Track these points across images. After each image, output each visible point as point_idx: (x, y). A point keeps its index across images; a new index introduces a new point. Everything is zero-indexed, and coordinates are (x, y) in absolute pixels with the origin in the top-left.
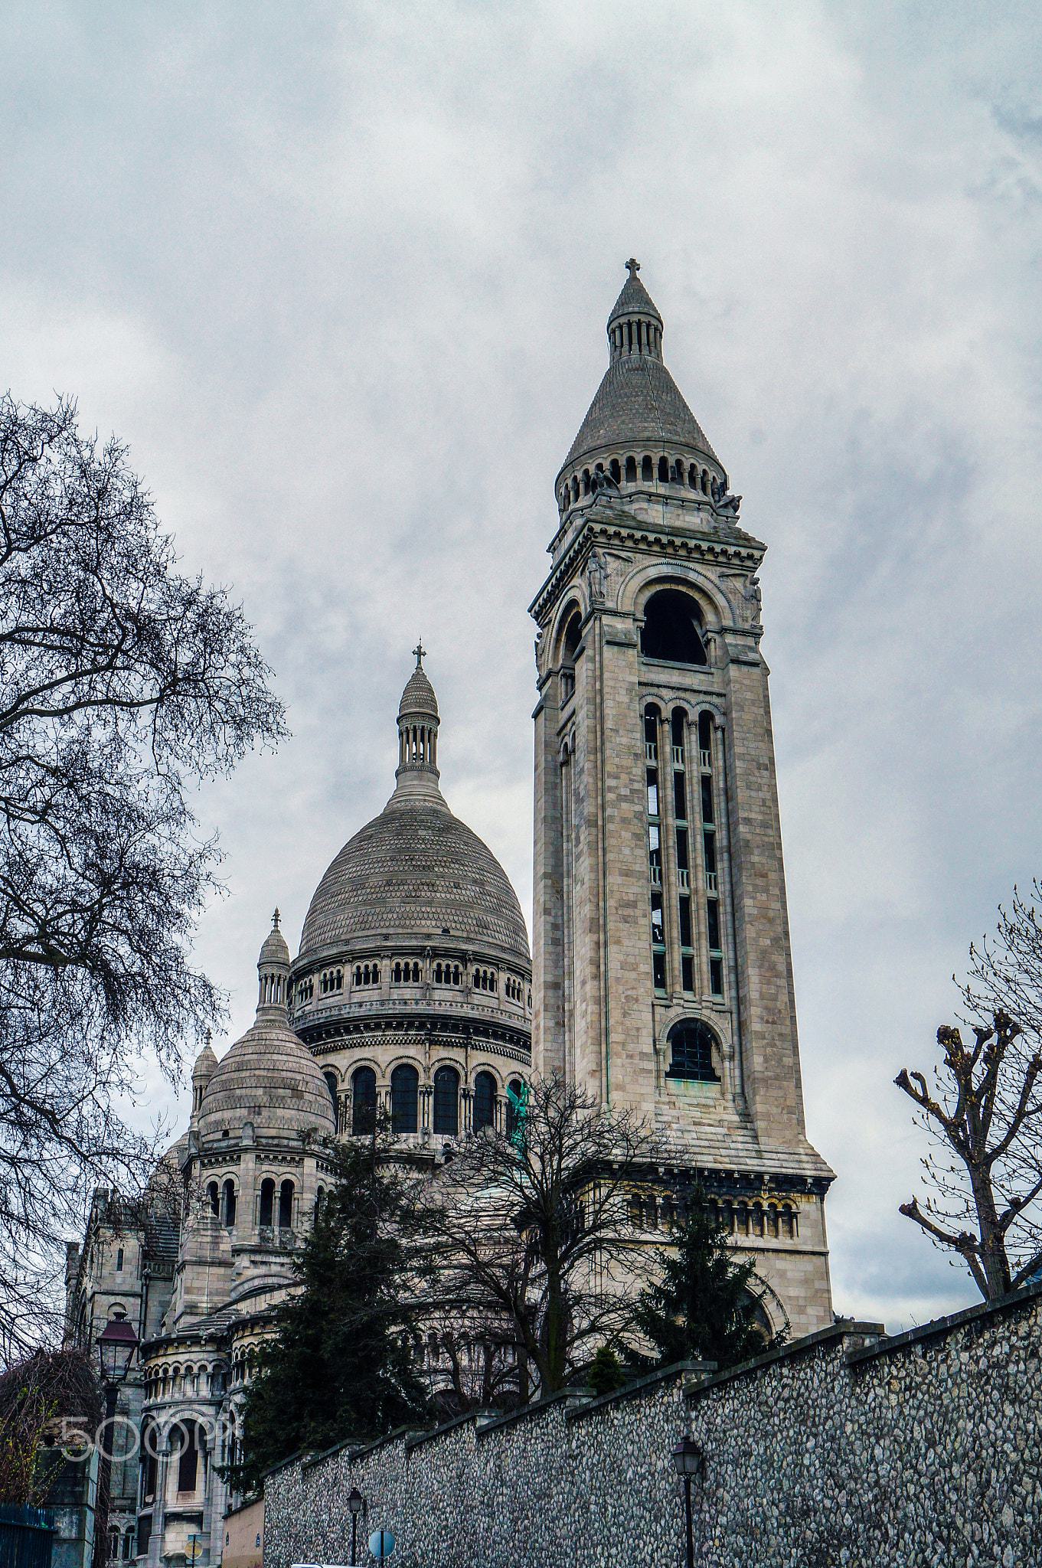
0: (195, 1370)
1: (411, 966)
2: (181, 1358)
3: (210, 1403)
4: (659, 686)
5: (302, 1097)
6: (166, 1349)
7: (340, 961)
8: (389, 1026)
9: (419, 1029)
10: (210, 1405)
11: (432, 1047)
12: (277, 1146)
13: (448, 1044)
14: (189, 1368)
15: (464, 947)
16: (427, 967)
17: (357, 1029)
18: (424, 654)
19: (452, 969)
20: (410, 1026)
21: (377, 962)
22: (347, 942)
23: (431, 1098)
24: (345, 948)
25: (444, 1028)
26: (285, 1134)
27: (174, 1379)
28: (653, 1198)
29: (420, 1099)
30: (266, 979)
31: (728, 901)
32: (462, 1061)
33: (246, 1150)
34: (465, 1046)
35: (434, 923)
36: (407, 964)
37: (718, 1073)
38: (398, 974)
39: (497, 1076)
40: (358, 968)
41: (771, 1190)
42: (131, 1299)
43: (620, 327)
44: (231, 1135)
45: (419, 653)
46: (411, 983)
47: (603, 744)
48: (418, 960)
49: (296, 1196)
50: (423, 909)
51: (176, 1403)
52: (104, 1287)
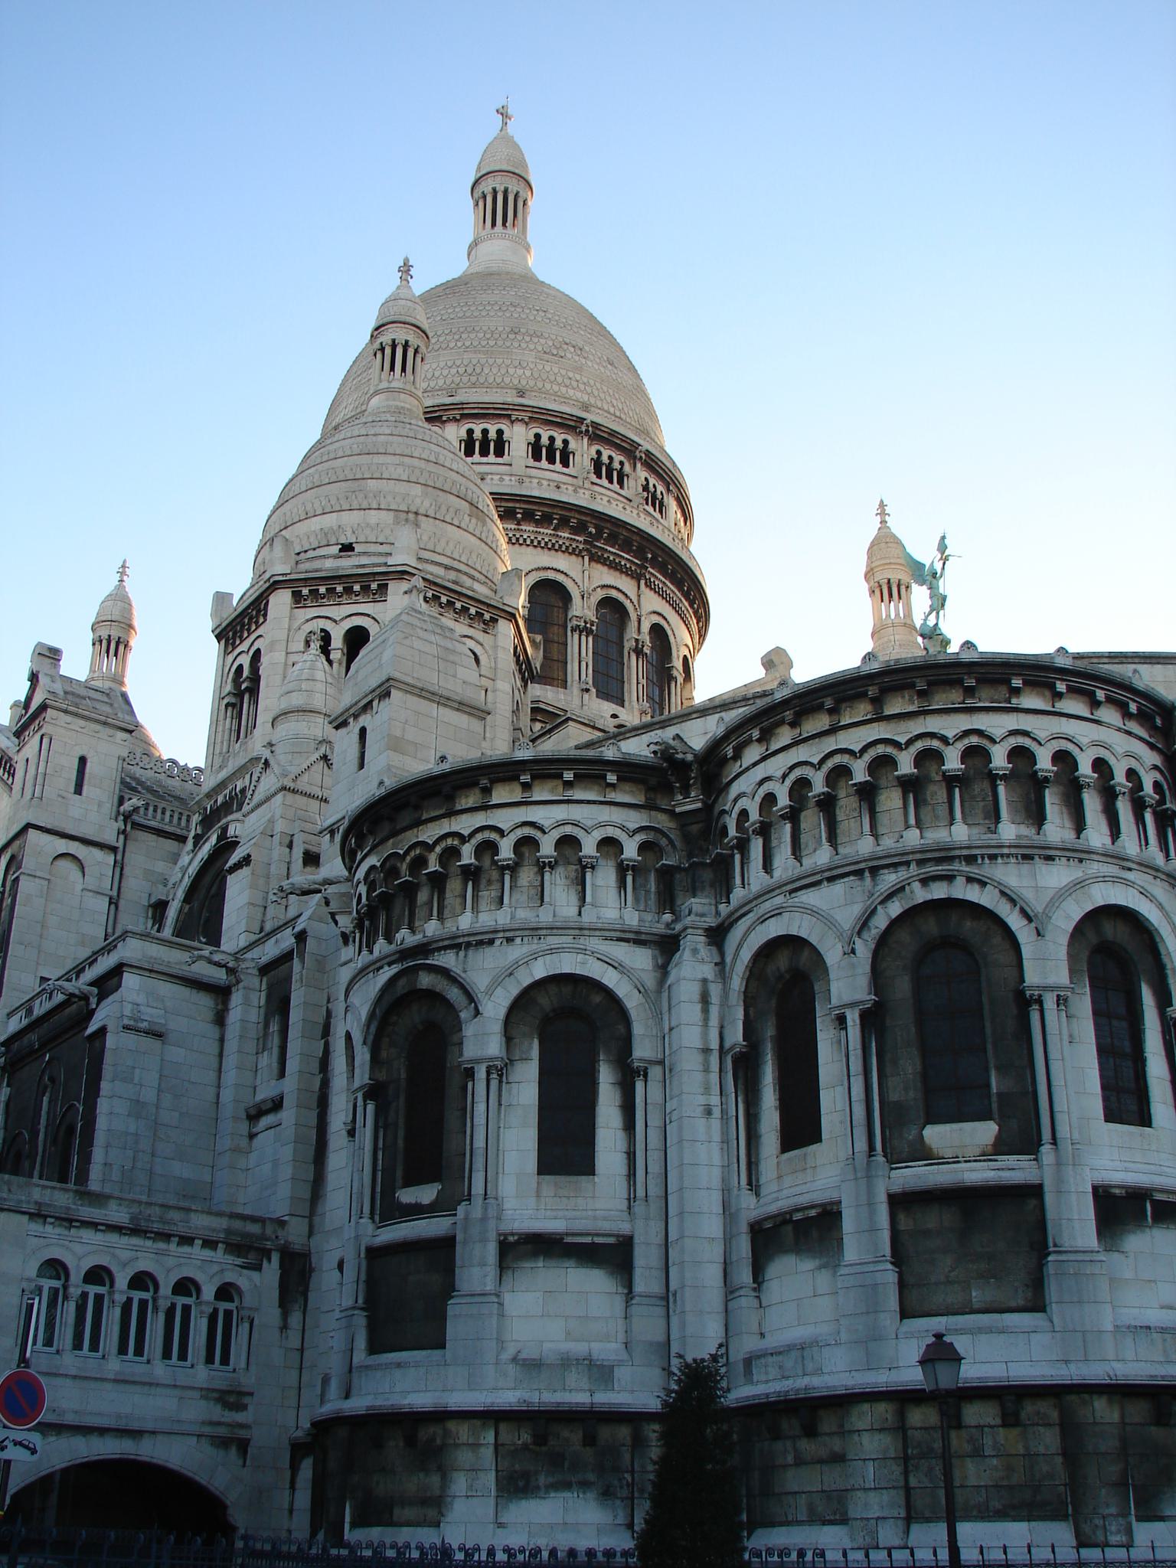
0: (589, 847)
1: (559, 444)
3: (638, 939)
5: (484, 524)
6: (487, 791)
8: (528, 516)
9: (575, 531)
11: (593, 564)
12: (455, 582)
13: (614, 566)
14: (569, 843)
16: (583, 451)
19: (616, 465)
20: (564, 523)
23: (590, 639)
25: (612, 539)
27: (514, 868)
29: (573, 640)
32: (635, 600)
33: (402, 575)
34: (637, 577)
36: (552, 439)
40: (470, 432)
42: (96, 852)
44: (358, 548)
46: (558, 466)
48: (569, 438)
50: (571, 374)
51: (535, 931)
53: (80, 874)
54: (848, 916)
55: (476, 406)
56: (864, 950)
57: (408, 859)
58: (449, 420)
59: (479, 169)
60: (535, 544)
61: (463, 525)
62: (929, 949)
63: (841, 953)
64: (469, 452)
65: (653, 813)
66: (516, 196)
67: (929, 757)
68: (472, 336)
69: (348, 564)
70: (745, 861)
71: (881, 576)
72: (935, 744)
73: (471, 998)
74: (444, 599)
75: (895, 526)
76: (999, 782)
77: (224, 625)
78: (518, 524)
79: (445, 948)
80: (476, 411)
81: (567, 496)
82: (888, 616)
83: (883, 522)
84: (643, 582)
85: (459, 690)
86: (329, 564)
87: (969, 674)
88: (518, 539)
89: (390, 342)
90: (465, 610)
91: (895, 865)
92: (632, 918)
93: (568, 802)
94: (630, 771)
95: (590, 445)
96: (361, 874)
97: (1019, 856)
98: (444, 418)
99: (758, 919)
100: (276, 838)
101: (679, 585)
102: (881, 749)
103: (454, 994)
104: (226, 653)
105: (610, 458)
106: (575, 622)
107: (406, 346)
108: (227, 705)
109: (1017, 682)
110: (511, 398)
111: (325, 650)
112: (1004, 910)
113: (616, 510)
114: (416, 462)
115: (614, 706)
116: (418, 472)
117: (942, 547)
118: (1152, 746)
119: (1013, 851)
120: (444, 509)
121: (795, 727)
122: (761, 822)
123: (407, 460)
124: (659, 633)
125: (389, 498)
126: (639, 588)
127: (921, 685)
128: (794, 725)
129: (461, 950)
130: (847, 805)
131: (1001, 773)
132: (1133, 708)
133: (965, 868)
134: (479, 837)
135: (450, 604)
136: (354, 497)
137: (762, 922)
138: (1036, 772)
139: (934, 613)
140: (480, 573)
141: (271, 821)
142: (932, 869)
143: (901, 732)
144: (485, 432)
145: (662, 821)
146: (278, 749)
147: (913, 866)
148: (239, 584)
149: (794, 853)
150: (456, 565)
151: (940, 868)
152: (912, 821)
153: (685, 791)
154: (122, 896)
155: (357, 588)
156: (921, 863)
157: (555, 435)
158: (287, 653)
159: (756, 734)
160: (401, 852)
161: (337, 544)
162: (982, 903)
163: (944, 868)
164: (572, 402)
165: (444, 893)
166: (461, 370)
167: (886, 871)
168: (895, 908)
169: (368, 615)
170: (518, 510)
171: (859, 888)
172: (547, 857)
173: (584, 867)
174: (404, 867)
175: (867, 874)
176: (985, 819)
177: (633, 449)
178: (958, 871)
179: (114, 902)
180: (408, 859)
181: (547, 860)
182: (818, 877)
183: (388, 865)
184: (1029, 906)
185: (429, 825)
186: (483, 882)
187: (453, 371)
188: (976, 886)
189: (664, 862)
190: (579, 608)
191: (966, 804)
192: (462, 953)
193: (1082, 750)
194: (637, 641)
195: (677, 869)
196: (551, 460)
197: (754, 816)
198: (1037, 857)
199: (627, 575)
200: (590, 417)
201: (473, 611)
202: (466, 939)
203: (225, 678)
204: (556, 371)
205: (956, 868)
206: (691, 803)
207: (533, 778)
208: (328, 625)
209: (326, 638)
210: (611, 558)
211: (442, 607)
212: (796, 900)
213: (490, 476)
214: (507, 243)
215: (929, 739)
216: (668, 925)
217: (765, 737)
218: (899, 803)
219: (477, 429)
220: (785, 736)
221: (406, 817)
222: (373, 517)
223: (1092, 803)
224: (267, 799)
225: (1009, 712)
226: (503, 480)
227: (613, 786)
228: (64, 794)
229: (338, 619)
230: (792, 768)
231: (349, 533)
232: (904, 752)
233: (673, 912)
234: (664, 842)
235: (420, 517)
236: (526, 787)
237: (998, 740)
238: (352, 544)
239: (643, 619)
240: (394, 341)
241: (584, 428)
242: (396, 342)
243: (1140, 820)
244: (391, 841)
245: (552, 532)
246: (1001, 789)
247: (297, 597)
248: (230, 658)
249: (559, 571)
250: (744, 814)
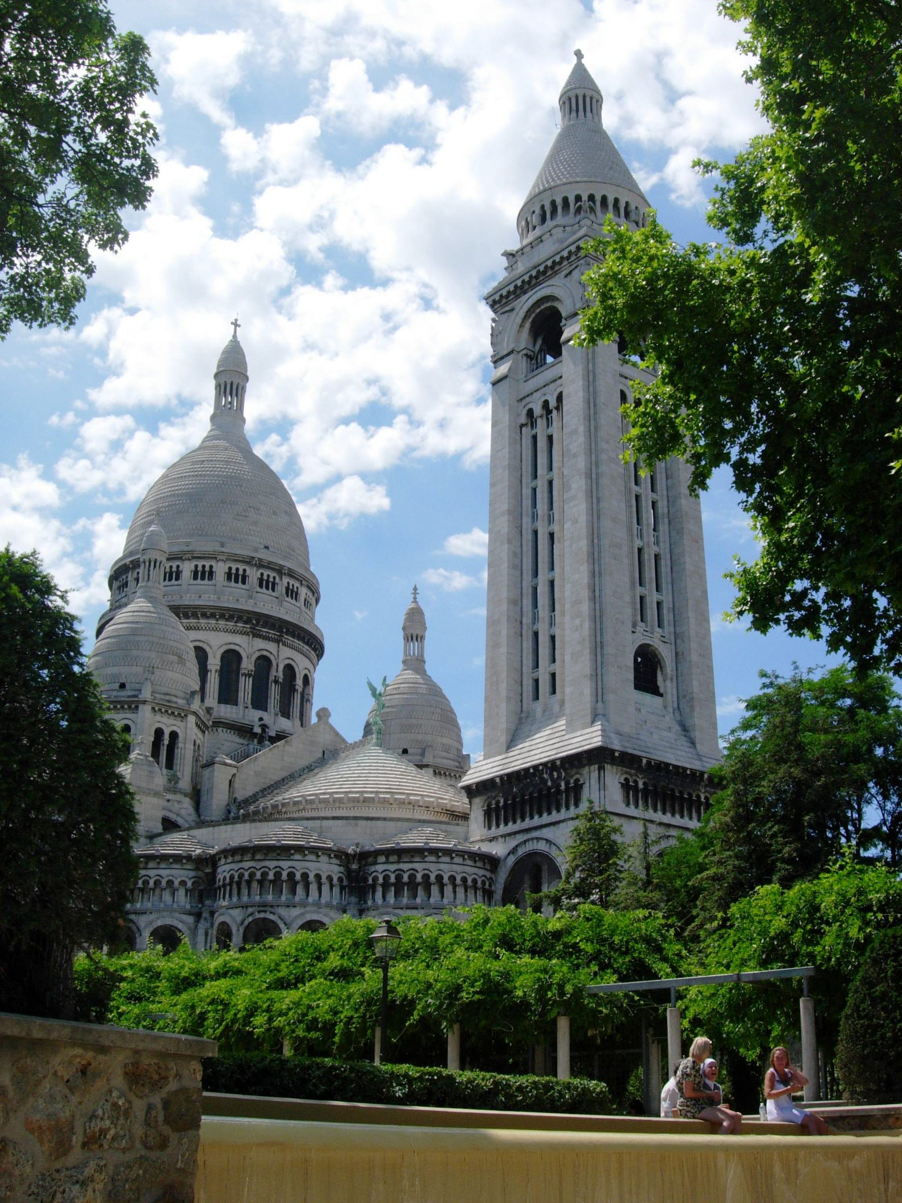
0: (176, 883)
1: (241, 572)
2: (162, 872)
3: (190, 914)
4: (626, 378)
5: (185, 665)
7: (181, 559)
8: (222, 616)
9: (246, 622)
11: (255, 639)
12: (169, 701)
14: (170, 883)
15: (282, 563)
16: (254, 574)
17: (195, 616)
18: (239, 326)
19: (271, 579)
20: (240, 619)
23: (251, 679)
24: (186, 549)
26: (173, 692)
27: (154, 890)
28: (636, 782)
29: (242, 680)
30: (150, 562)
31: (668, 556)
33: (144, 702)
34: (277, 642)
35: (258, 539)
36: (237, 569)
37: (662, 690)
38: (229, 575)
39: (297, 670)
40: (196, 566)
41: (706, 786)
43: (570, 99)
45: (236, 324)
46: (240, 585)
47: (595, 413)
49: (180, 745)
54: (239, 919)
56: (242, 930)
64: (195, 578)
67: (265, 875)
69: (124, 695)
73: (139, 930)
74: (163, 710)
83: (415, 598)
91: (252, 906)
95: (257, 570)
103: (134, 928)
105: (268, 576)
118: (340, 865)
124: (290, 670)
128: (232, 856)
132: (332, 856)
133: (270, 909)
143: (258, 865)
144: (204, 566)
145: (200, 874)
150: (170, 691)
168: (250, 919)
196: (236, 581)
200: (258, 555)
201: (176, 713)
206: (208, 870)
217: (226, 857)
219: (200, 564)
220: (230, 859)
222: (135, 669)
223: (313, 887)
243: (331, 889)
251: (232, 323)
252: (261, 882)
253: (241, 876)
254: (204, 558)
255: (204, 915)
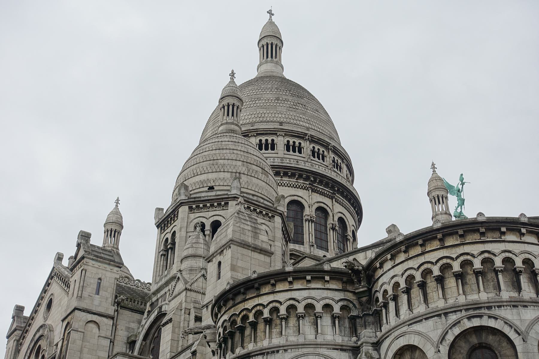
0: (319, 308)
1: (297, 144)
3: (342, 348)
5: (268, 177)
6: (274, 285)
8: (286, 174)
9: (306, 179)
10: (342, 350)
11: (313, 193)
12: (257, 201)
14: (309, 307)
16: (307, 146)
18: (273, 15)
19: (321, 152)
20: (300, 176)
21: (274, 138)
22: (252, 124)
23: (313, 224)
25: (321, 183)
27: (286, 319)
29: (306, 225)
32: (332, 209)
33: (235, 198)
36: (294, 142)
39: (347, 223)
40: (260, 141)
44: (216, 188)
45: (270, 13)
46: (297, 153)
50: (301, 116)
51: (297, 346)
52: (83, 305)
53: (98, 329)
54: (435, 336)
55: (263, 130)
56: (444, 349)
57: (241, 316)
58: (252, 136)
59: (260, 35)
60: (289, 185)
61: (259, 177)
62: (473, 349)
63: (434, 352)
64: (260, 148)
65: (346, 293)
66: (276, 46)
68: (260, 102)
70: (387, 312)
71: (435, 194)
72: (469, 257)
74: (252, 208)
75: (440, 173)
76: (499, 273)
77: (160, 221)
78: (282, 177)
79: (258, 355)
80: (263, 132)
81: (302, 165)
82: (439, 210)
84: (334, 200)
85: (260, 245)
86: (203, 195)
87: (482, 227)
88: (281, 184)
89: (227, 104)
90: (261, 212)
91: (455, 311)
92: (339, 340)
93: (309, 289)
94: (335, 275)
96: (220, 324)
97: (512, 306)
98: (250, 135)
99: (395, 338)
100: (183, 311)
101: (349, 201)
102: (445, 261)
104: (161, 233)
105: (319, 149)
106: (306, 217)
107: (233, 106)
108: (161, 255)
109: (503, 229)
110: (277, 126)
111: (203, 230)
112: (506, 330)
113: (321, 170)
114: (239, 152)
115: (324, 252)
116: (240, 156)
117: (462, 180)
119: (508, 304)
120: (251, 171)
121: (406, 253)
122: (394, 295)
123: (235, 152)
125: (228, 167)
126: (332, 203)
127: (461, 232)
128: (405, 252)
129: (264, 355)
130: (431, 284)
131: (500, 269)
133: (486, 311)
134: (271, 305)
135: (255, 210)
136: (213, 167)
137: (397, 339)
138: (515, 269)
139: (460, 207)
140: (267, 197)
141: (181, 303)
142: (471, 312)
143: (454, 253)
144: (267, 140)
145: (350, 296)
146: (183, 273)
147: (463, 311)
148: (166, 204)
149: (409, 308)
150: (256, 194)
151: (476, 312)
152: (461, 291)
153: (359, 282)
154: (115, 339)
155: (216, 204)
156: (466, 310)
157: (295, 140)
158: (187, 232)
159: (389, 256)
160: (238, 313)
161: (207, 187)
162: (496, 327)
163: (477, 312)
164: (302, 127)
165: (257, 330)
166: (256, 116)
167: (451, 314)
168: (457, 331)
169: (221, 216)
170: (281, 172)
171: (439, 322)
172: (301, 313)
173: (317, 317)
174: (239, 320)
175: (443, 316)
176: (494, 290)
177: (328, 145)
178: (484, 313)
179: (112, 342)
180: (241, 316)
181: (301, 315)
182: (421, 318)
183: (232, 319)
184: (518, 328)
185: (249, 301)
186: (274, 325)
187: (253, 116)
188: (493, 320)
189: (352, 314)
190: (308, 212)
191: (485, 284)
192: (265, 357)
193: (535, 258)
194: (333, 224)
195: (358, 317)
196: (294, 151)
197: (390, 292)
198: (519, 306)
199: (328, 197)
200: (309, 133)
201: (264, 213)
202: (267, 351)
203: (160, 244)
204: (295, 115)
205: (483, 312)
207: (294, 279)
208: (204, 220)
209: (203, 226)
210: (321, 190)
211: (251, 212)
212: (411, 328)
213: (269, 158)
214: (273, 64)
215: (466, 255)
216: (355, 343)
217: (393, 258)
218: (455, 284)
219: (263, 139)
220: (402, 257)
221: (239, 298)
222: (222, 175)
224: (179, 294)
225: (501, 242)
226: (275, 160)
227: (328, 281)
228: (91, 295)
229: (208, 217)
230: (406, 271)
231: (212, 182)
232: (455, 262)
233: (357, 336)
234: (351, 305)
235: (241, 175)
236: (291, 283)
237: (497, 255)
238: (213, 186)
239: (335, 215)
240: (228, 103)
241: (307, 137)
242: (230, 104)
244: (233, 308)
245: (296, 180)
246: (500, 276)
247: (191, 208)
248: (163, 235)
249: (299, 196)
250: (386, 291)
251: (268, 12)
252: (460, 276)
253: (427, 273)
254: (266, 134)
255: (364, 349)
